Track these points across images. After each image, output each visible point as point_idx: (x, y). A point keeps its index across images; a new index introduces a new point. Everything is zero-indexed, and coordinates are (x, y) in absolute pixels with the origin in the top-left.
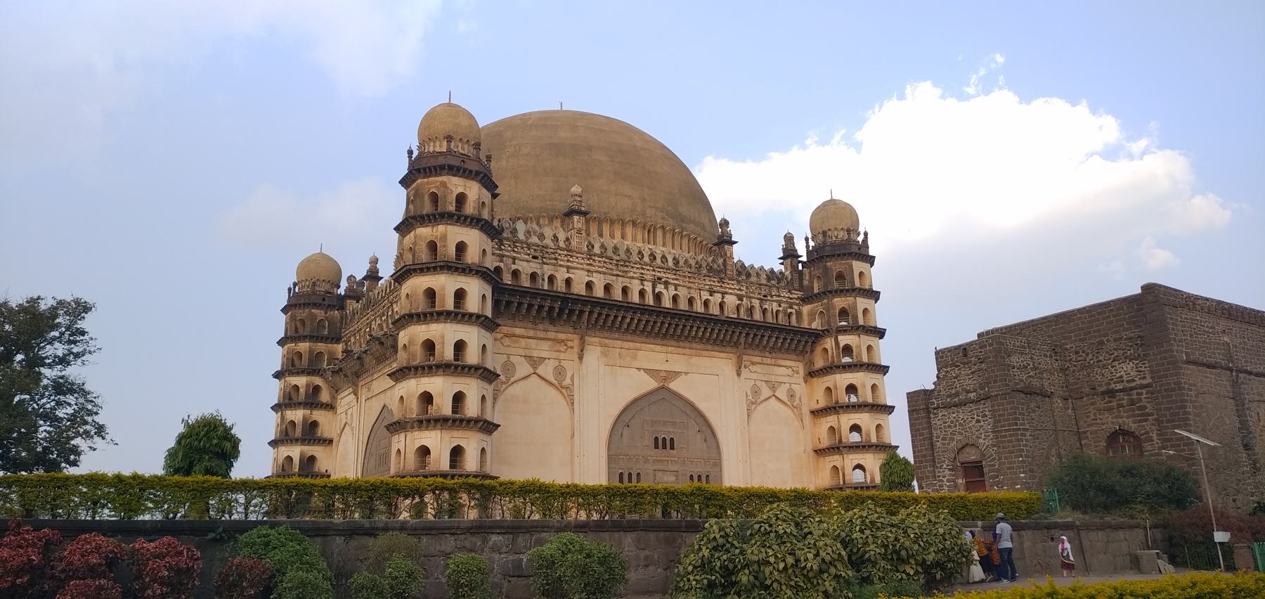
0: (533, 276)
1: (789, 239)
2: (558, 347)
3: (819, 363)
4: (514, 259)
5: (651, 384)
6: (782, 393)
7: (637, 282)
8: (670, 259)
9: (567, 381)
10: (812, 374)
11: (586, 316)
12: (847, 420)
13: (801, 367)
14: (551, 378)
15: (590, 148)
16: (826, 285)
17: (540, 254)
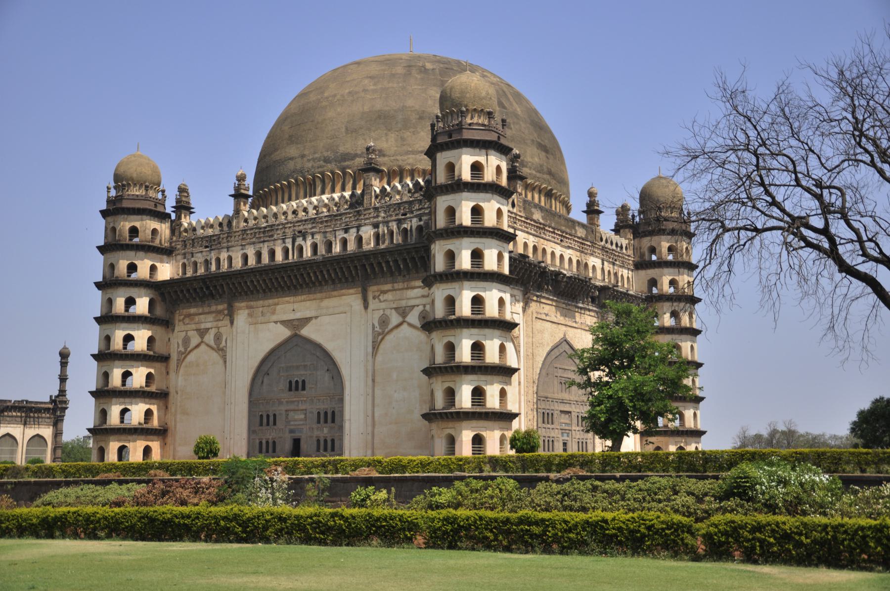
6: (413, 318)
7: (280, 241)
9: (223, 343)
14: (212, 343)
17: (211, 243)
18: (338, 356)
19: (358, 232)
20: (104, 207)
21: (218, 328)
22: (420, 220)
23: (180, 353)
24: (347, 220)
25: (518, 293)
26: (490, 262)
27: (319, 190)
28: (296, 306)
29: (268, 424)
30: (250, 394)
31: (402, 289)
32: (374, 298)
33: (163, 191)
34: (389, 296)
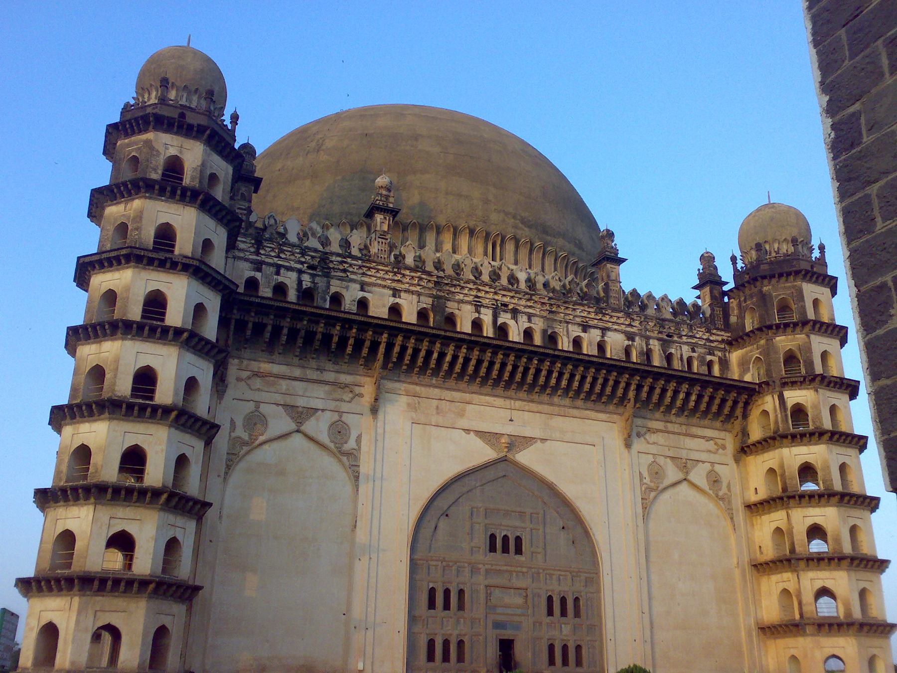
0: (306, 295)
1: (708, 260)
2: (339, 393)
3: (756, 433)
4: (278, 267)
5: (485, 453)
6: (699, 475)
9: (351, 444)
10: (745, 449)
11: (382, 349)
12: (803, 517)
13: (730, 441)
14: (324, 438)
15: (416, 137)
16: (762, 317)
19: (603, 337)
21: (340, 413)
22: (693, 351)
23: (236, 442)
24: (585, 314)
28: (516, 414)
29: (447, 606)
30: (413, 548)
31: (679, 434)
32: (639, 435)
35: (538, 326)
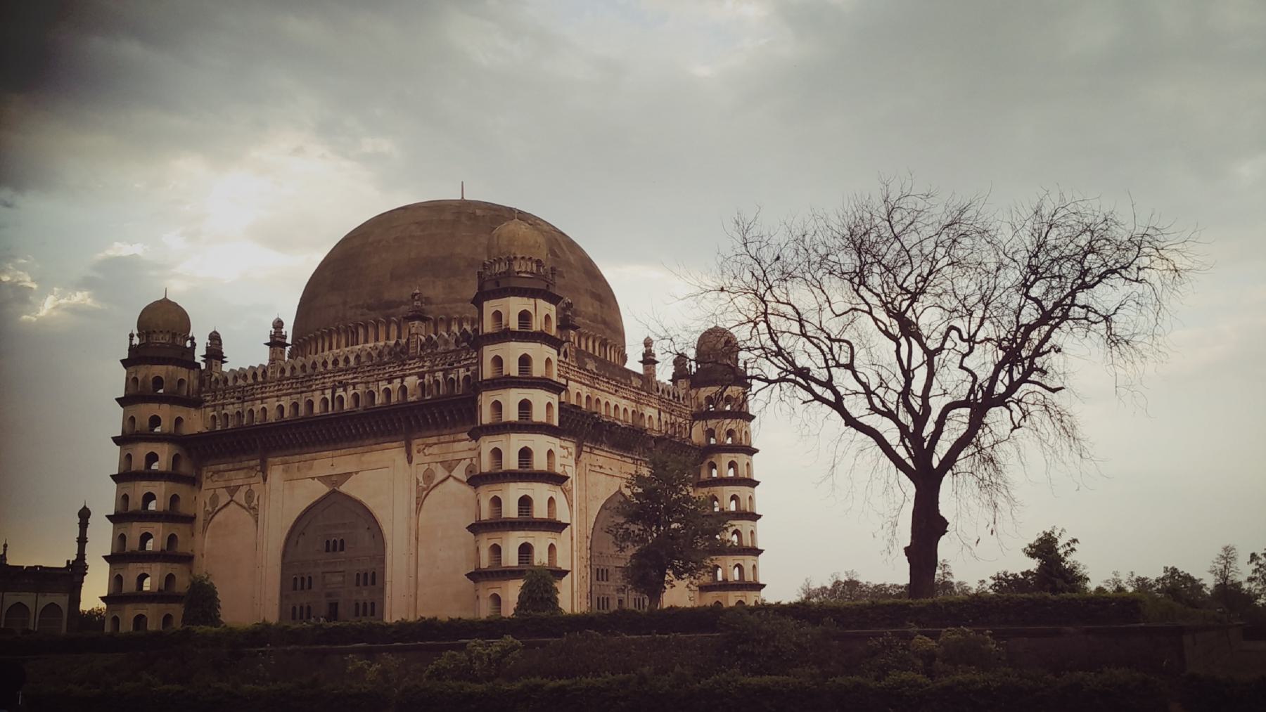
4: (223, 405)
5: (323, 489)
6: (460, 472)
7: (319, 393)
8: (352, 359)
14: (243, 503)
18: (378, 514)
20: (126, 357)
25: (572, 447)
26: (538, 415)
27: (361, 338)
32: (419, 452)
33: (192, 339)
34: (435, 450)
35: (360, 389)
